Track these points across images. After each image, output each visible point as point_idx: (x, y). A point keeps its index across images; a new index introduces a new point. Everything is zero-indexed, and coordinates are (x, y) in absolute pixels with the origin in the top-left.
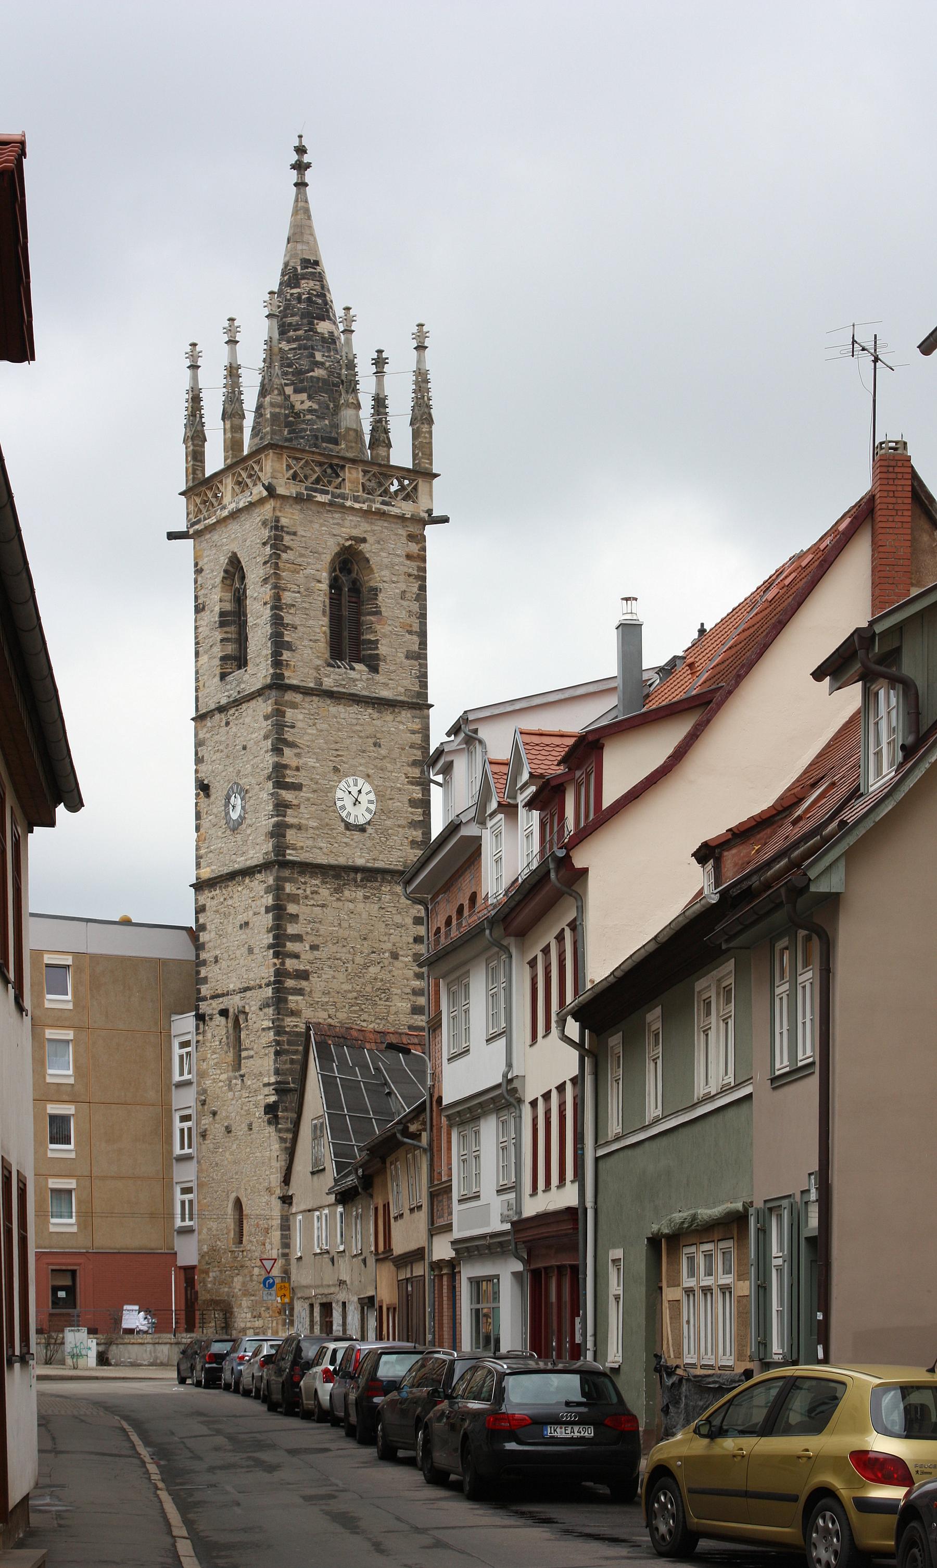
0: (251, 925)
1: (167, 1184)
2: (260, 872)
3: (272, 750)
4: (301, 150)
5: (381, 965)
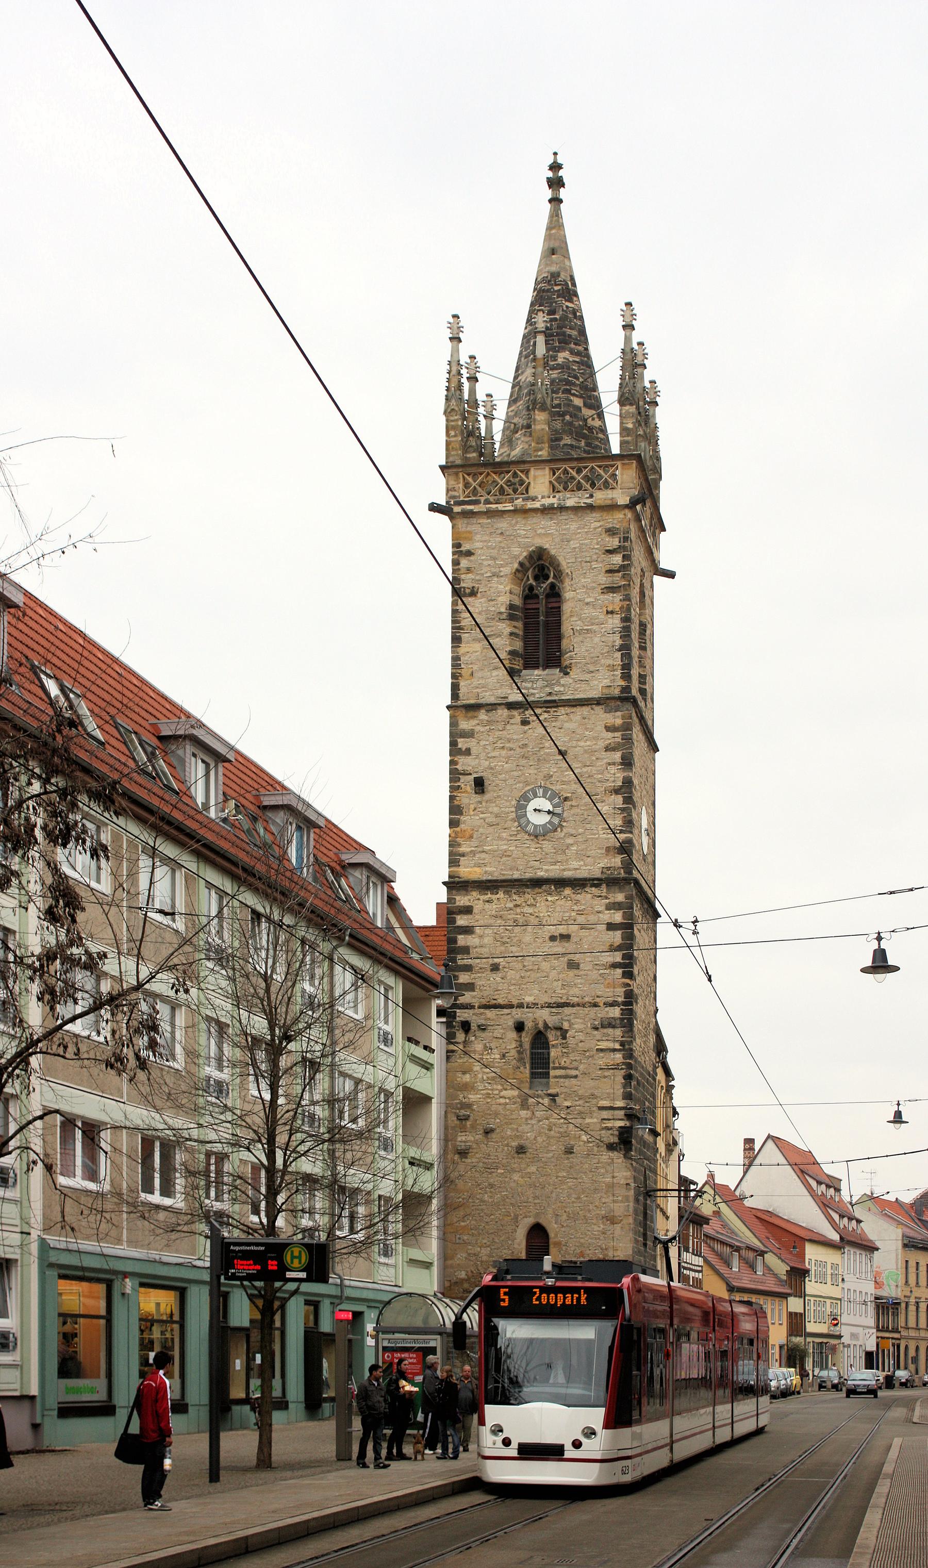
2: (596, 886)
3: (622, 764)
4: (555, 167)
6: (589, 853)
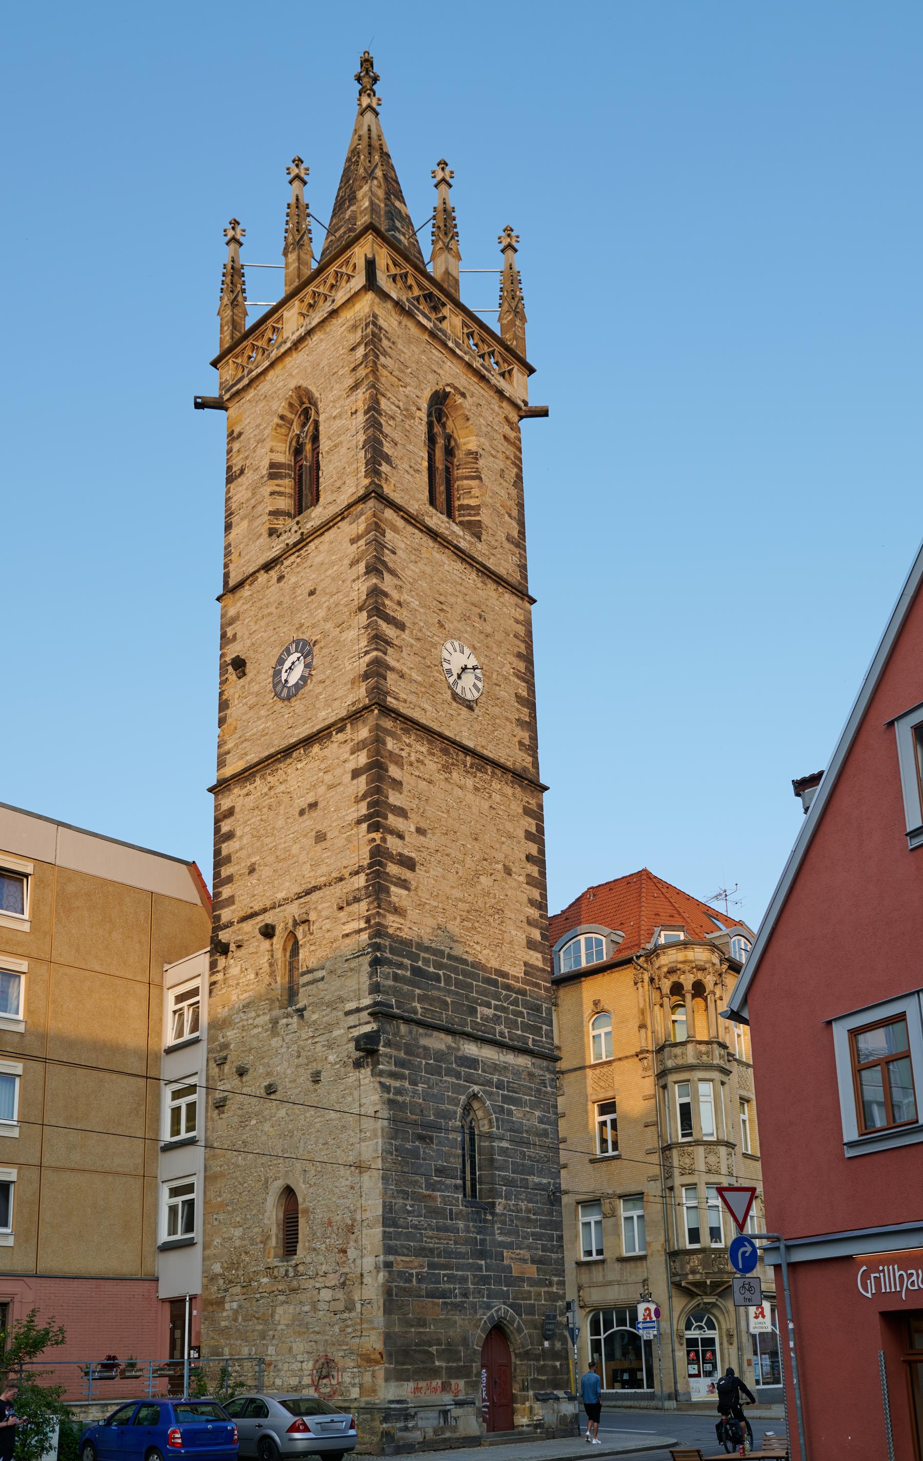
0: (320, 806)
1: (147, 1181)
5: (493, 877)
6: (336, 696)
